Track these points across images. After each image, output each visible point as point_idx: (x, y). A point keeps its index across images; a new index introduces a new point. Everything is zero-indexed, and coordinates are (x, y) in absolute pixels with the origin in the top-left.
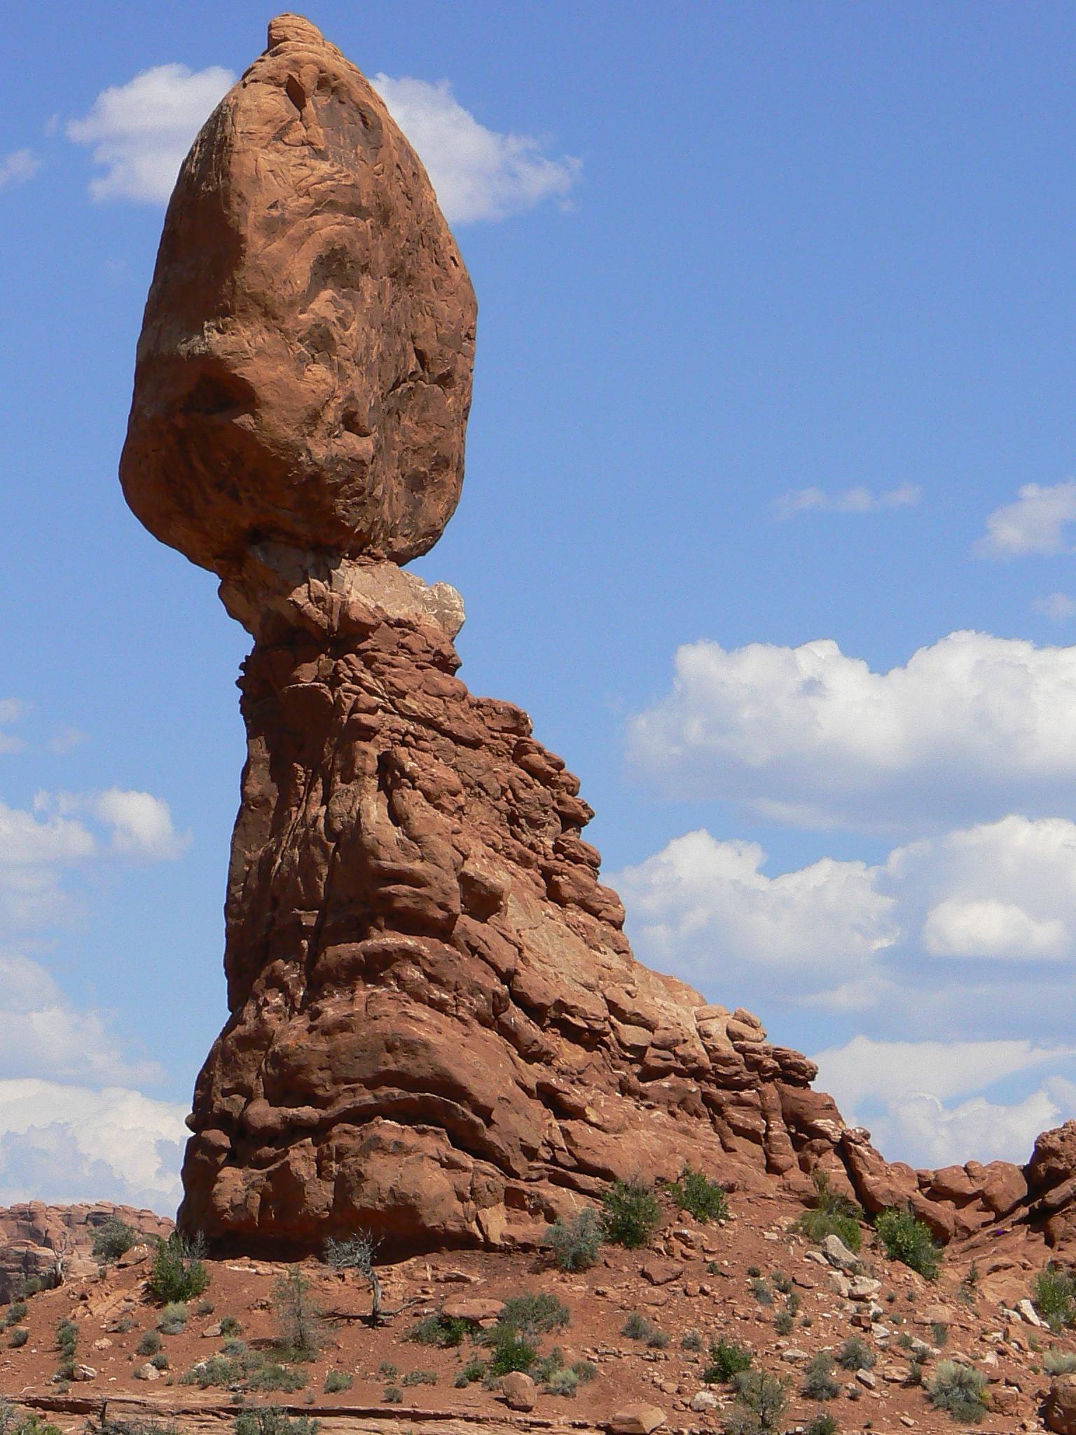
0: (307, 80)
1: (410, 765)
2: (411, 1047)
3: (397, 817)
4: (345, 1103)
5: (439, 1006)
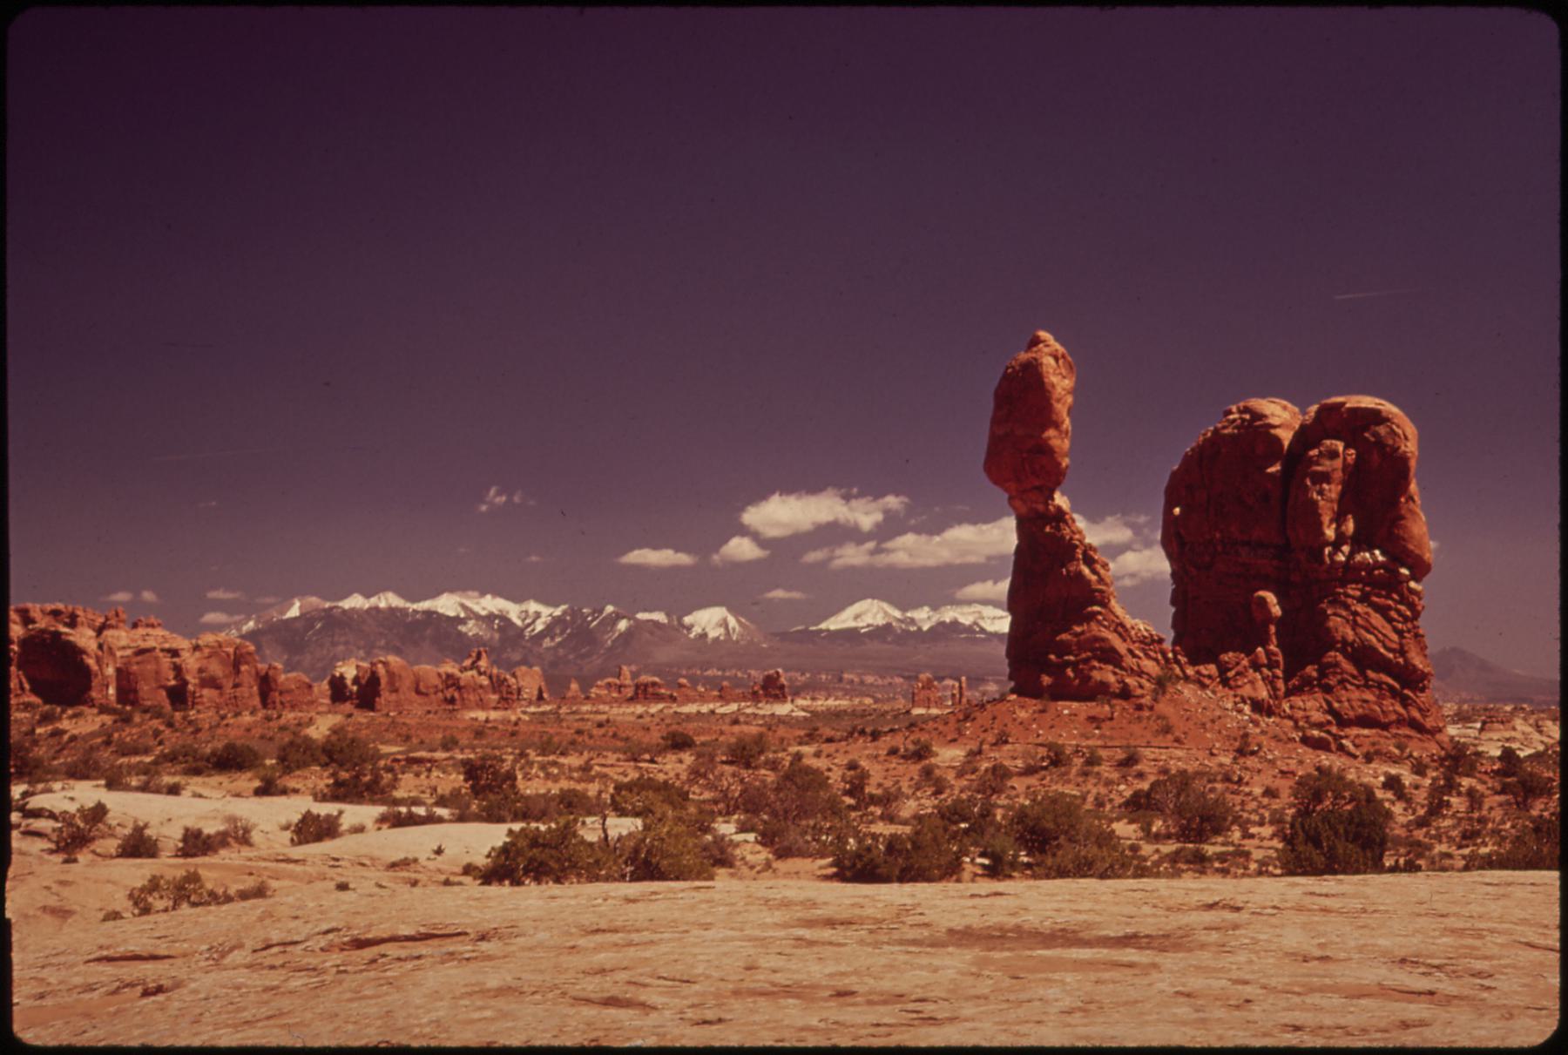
0: (1060, 356)
1: (1096, 557)
2: (1104, 640)
3: (1094, 572)
4: (1084, 656)
5: (1105, 627)
